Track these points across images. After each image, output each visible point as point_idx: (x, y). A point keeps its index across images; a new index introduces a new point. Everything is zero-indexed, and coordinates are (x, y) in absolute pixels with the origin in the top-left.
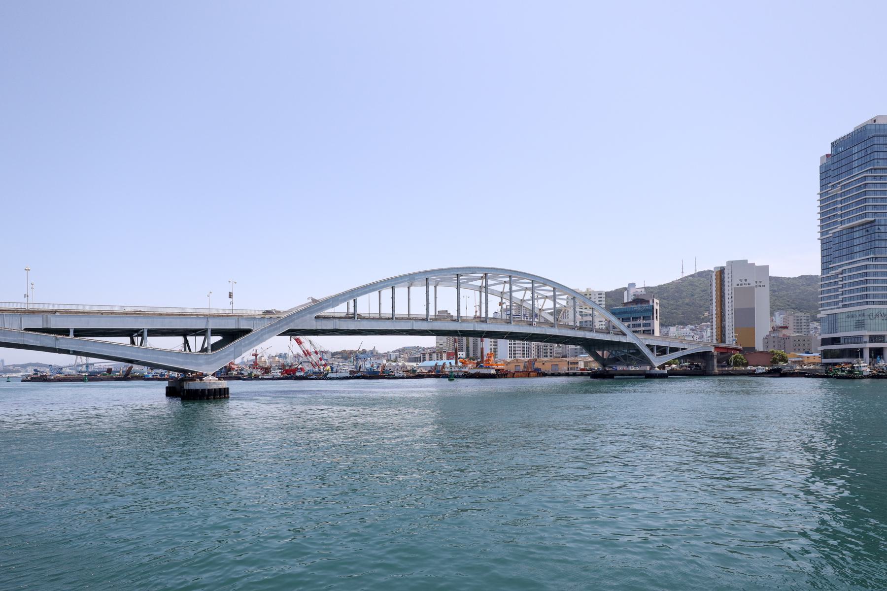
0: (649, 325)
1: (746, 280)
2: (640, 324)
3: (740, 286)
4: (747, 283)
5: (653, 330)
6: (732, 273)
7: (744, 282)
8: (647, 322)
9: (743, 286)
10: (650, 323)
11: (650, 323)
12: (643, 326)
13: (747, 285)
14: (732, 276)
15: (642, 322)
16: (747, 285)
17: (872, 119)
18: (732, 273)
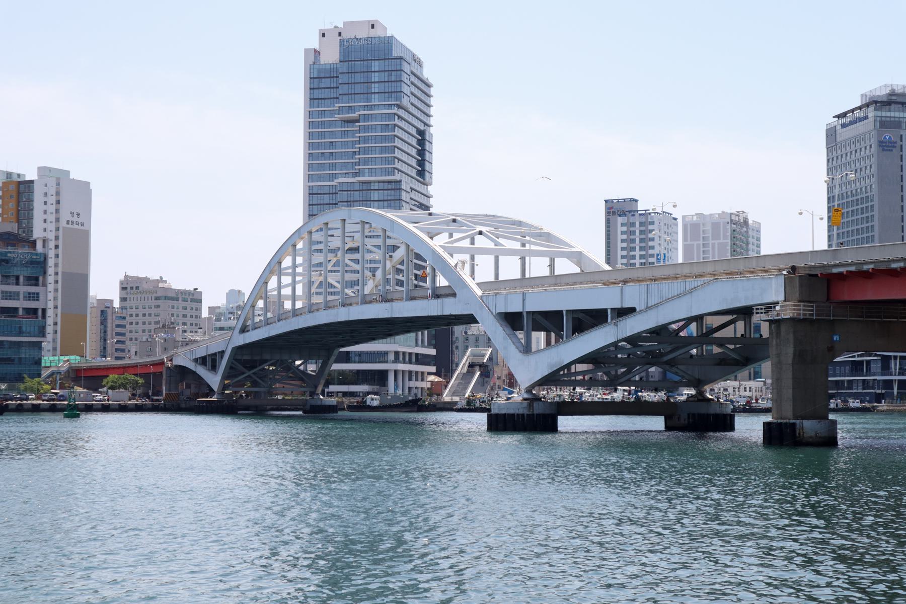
0: (35, 297)
1: (78, 215)
2: (18, 293)
3: (70, 226)
4: (80, 220)
5: (44, 311)
6: (58, 193)
7: (75, 219)
8: (33, 289)
9: (75, 226)
10: (38, 294)
11: (38, 294)
12: (25, 298)
13: (80, 227)
14: (58, 202)
15: (23, 289)
16: (80, 227)
17: (369, 21)
18: (58, 193)
